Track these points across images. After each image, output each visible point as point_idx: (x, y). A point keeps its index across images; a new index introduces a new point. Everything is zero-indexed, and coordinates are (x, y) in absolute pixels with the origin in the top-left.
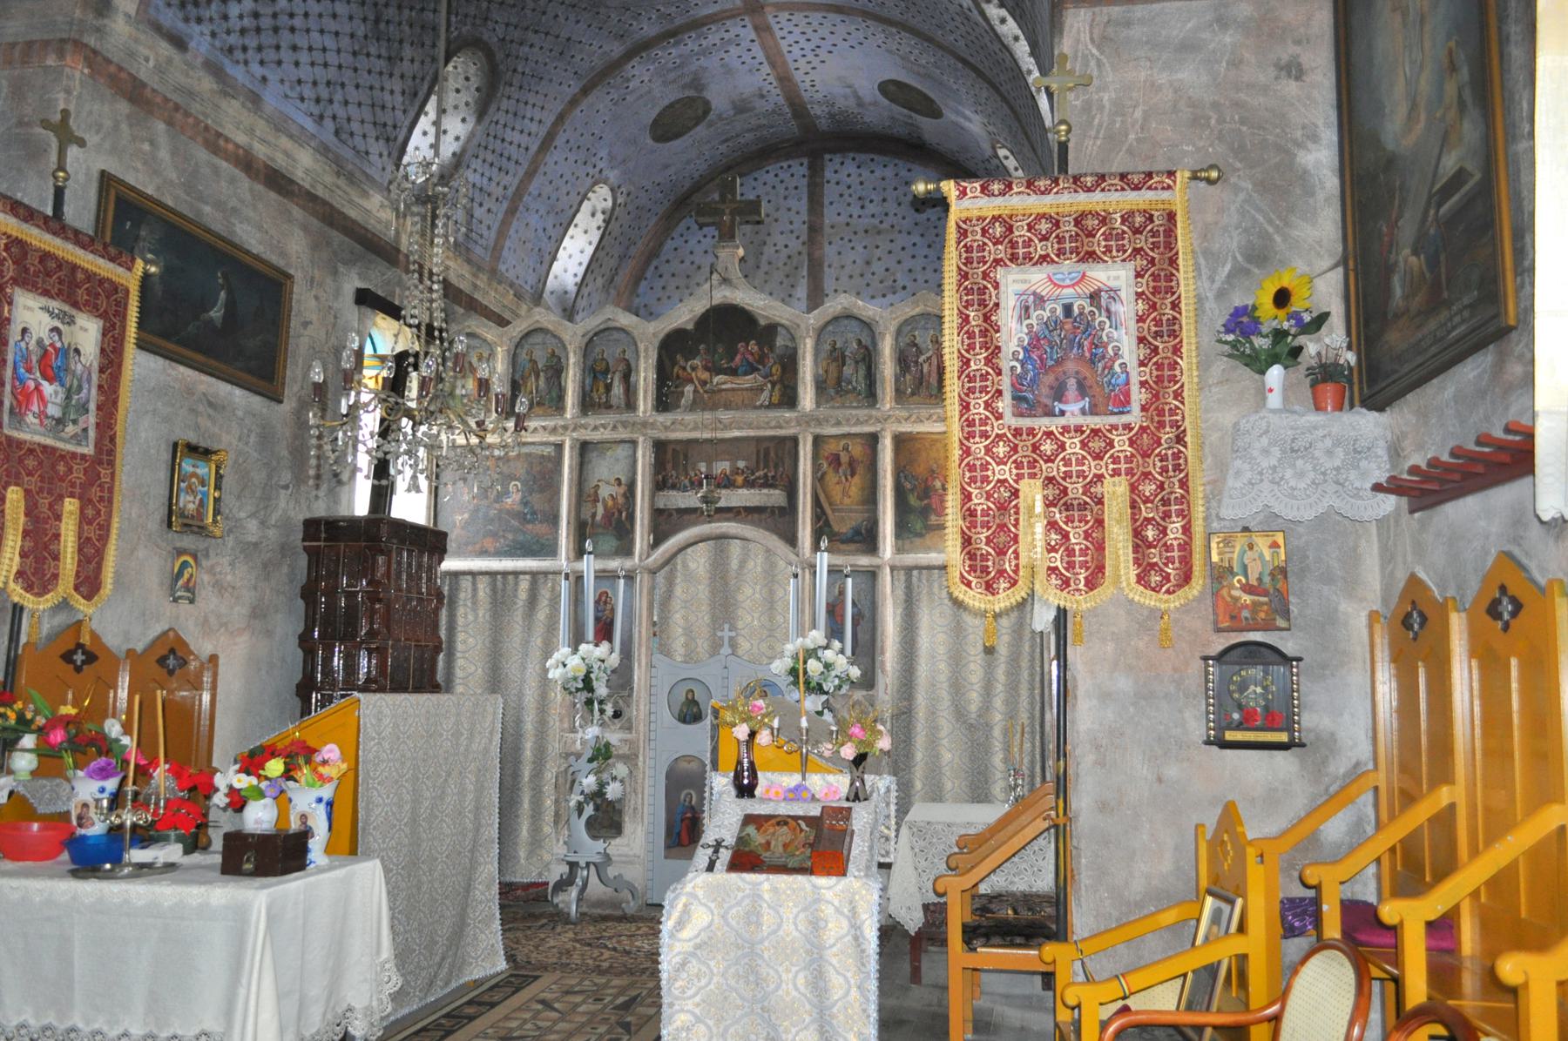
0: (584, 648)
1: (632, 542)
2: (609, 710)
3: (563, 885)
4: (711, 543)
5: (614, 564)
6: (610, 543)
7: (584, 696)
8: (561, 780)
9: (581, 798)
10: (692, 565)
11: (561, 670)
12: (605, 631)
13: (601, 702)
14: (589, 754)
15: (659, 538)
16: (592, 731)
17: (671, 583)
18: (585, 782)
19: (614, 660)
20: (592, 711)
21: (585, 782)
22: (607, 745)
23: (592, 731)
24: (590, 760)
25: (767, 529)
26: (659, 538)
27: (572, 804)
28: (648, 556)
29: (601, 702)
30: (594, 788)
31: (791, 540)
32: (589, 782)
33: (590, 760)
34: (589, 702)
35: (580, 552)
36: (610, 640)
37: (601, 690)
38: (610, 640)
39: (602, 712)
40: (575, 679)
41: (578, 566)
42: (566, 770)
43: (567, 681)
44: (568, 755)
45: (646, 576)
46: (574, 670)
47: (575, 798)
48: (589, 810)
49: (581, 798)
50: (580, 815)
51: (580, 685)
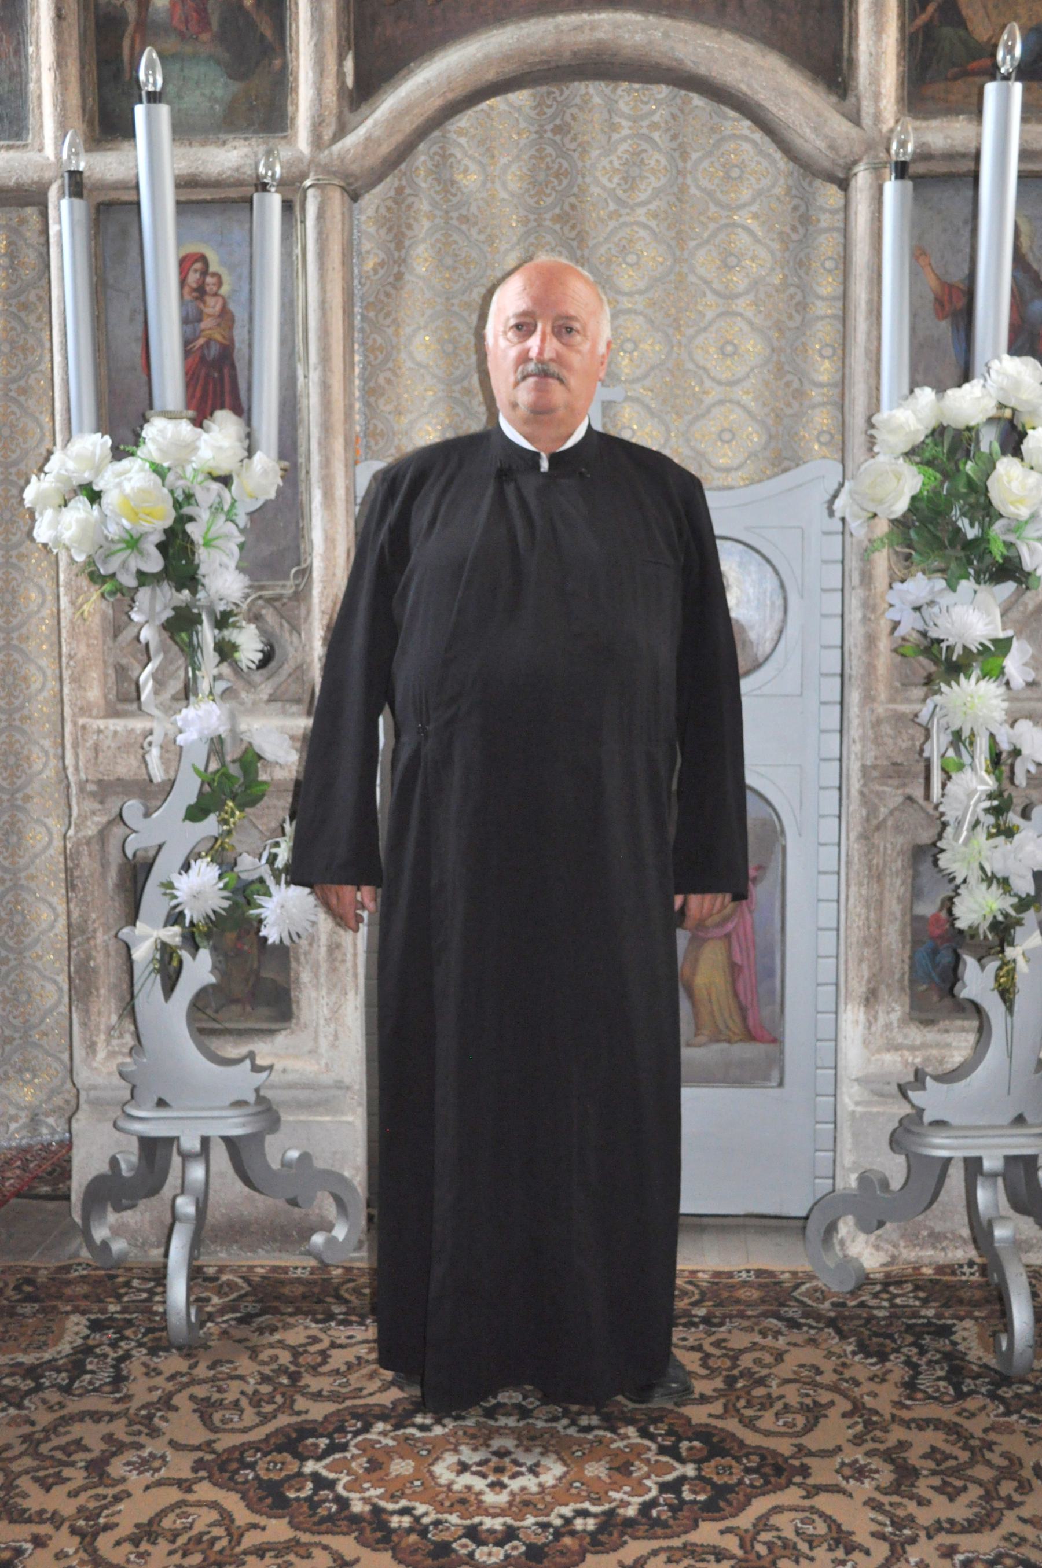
0: (159, 433)
1: (282, 84)
2: (249, 644)
3: (111, 1191)
4: (521, 98)
5: (228, 157)
6: (212, 87)
7: (166, 599)
8: (88, 864)
9: (172, 935)
10: (470, 180)
11: (80, 510)
12: (216, 385)
13: (222, 621)
14: (188, 790)
15: (372, 72)
16: (201, 720)
17: (397, 234)
18: (186, 885)
19: (263, 475)
20: (191, 651)
21: (186, 885)
22: (251, 760)
23: (201, 720)
24: (196, 813)
25: (746, 32)
26: (372, 72)
27: (142, 953)
28: (342, 130)
29: (222, 621)
30: (216, 901)
31: (833, 71)
32: (200, 887)
33: (196, 813)
34: (181, 624)
35: (108, 121)
36: (242, 410)
37: (224, 580)
38: (242, 410)
39: (225, 651)
40: (133, 542)
41: (105, 166)
42: (103, 835)
43: (105, 548)
44: (106, 789)
45: (336, 197)
46: (134, 508)
47: (148, 937)
48: (200, 969)
49: (172, 935)
50: (169, 985)
51: (154, 563)
